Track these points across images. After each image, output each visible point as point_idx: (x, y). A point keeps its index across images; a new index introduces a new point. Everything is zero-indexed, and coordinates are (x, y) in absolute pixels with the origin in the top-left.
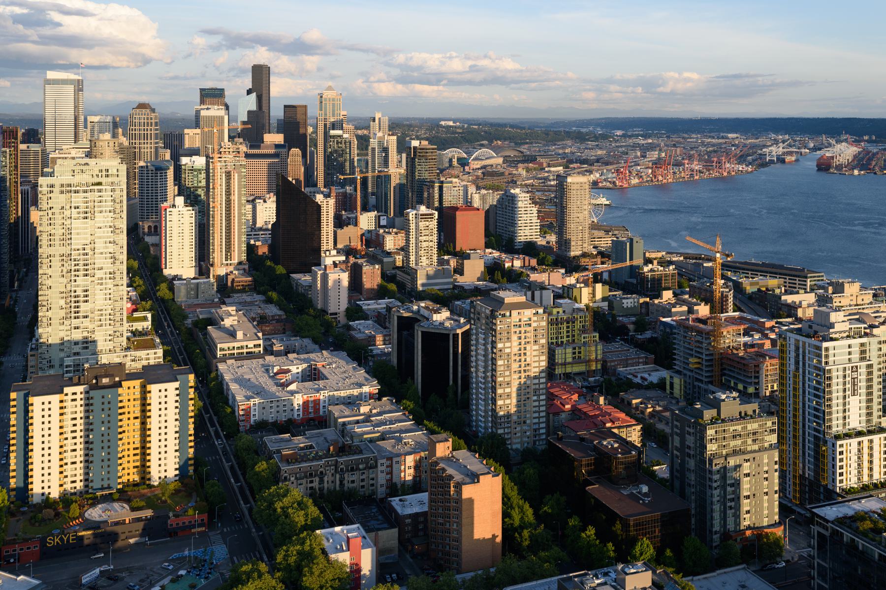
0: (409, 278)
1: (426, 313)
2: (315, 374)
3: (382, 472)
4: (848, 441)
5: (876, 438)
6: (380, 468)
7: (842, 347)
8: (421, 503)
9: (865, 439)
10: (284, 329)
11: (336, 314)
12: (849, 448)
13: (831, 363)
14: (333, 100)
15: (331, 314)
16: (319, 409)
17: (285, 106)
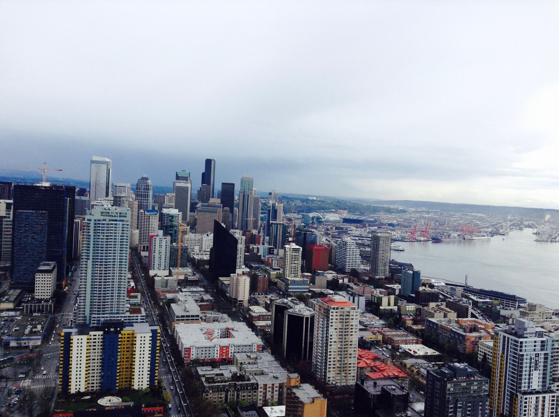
0: (284, 283)
1: (291, 304)
2: (228, 334)
3: (261, 392)
4: (530, 396)
5: (547, 396)
6: (260, 390)
7: (530, 342)
8: (281, 411)
9: (541, 396)
10: (213, 308)
11: (242, 301)
12: (531, 400)
13: (523, 350)
14: (249, 182)
15: (240, 301)
16: (228, 354)
17: (223, 184)
